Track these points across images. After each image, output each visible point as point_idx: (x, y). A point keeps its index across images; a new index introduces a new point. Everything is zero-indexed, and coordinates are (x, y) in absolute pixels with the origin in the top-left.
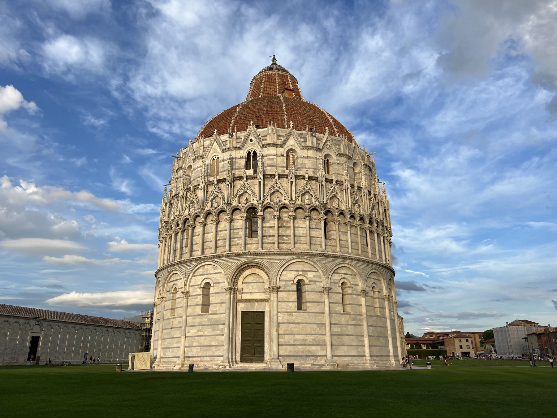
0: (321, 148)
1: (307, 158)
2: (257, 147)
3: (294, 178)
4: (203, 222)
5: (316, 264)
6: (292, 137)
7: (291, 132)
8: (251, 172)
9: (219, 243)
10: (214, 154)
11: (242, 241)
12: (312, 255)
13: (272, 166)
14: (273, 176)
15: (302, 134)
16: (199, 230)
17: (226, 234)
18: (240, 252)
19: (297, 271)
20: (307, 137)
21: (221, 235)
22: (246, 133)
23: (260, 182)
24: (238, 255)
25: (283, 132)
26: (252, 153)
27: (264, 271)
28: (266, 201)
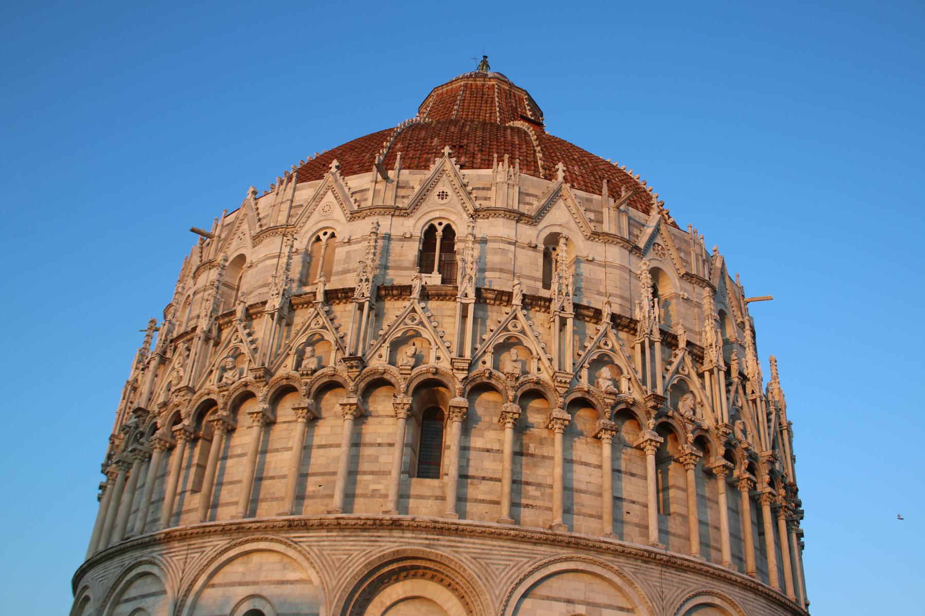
0: (642, 246)
1: (604, 265)
2: (458, 214)
3: (570, 309)
4: (263, 413)
5: (631, 584)
6: (561, 203)
7: (560, 189)
8: (434, 279)
9: (312, 485)
10: (321, 225)
11: (389, 485)
12: (623, 553)
13: (501, 270)
14: (504, 297)
15: (589, 200)
16: (246, 436)
17: (337, 459)
18: (380, 516)
19: (569, 601)
20: (605, 211)
21: (319, 459)
22: (428, 174)
23: (465, 307)
24: (376, 525)
25: (538, 186)
26: (440, 229)
27: (455, 590)
28: (480, 367)
